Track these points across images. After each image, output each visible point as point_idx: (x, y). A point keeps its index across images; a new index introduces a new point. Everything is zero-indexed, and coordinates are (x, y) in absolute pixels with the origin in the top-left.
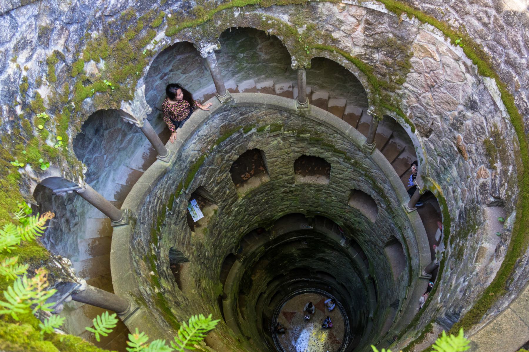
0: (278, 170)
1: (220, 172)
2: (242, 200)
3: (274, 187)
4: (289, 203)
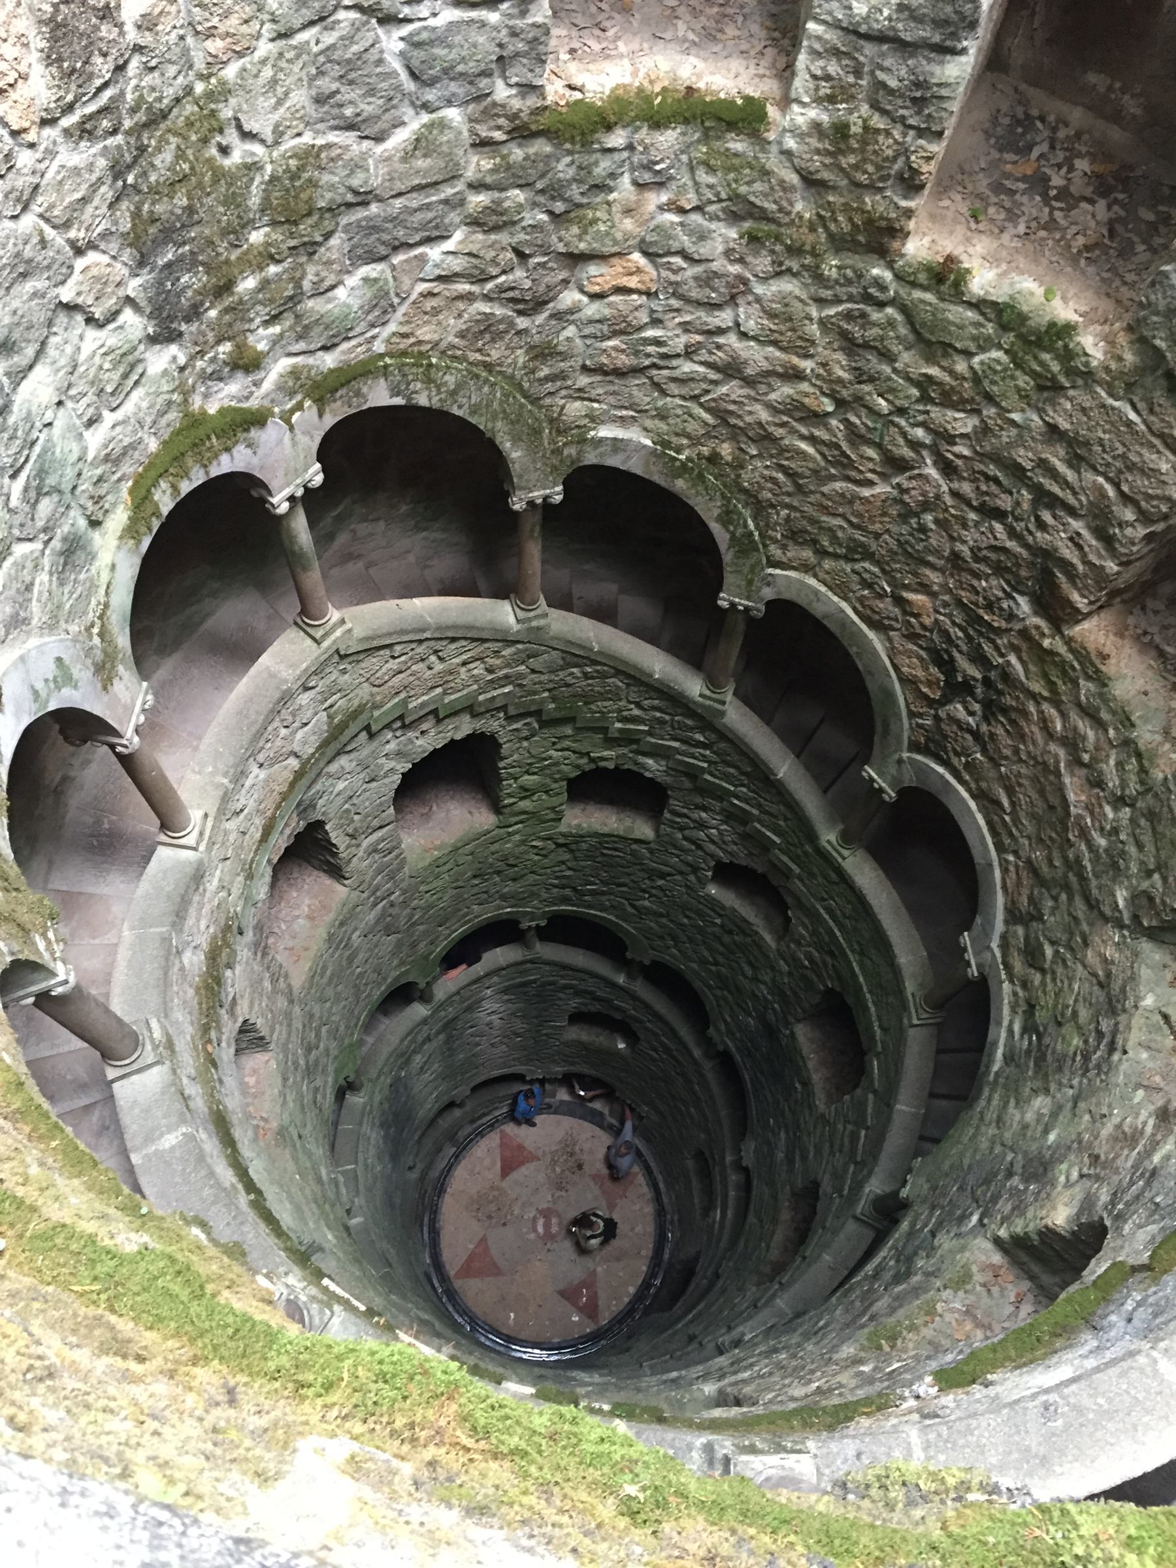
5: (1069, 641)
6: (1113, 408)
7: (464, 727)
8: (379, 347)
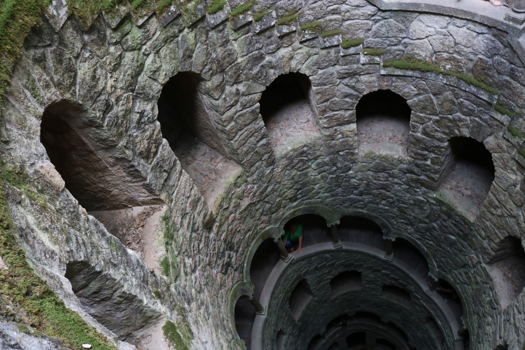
0: (488, 223)
1: (437, 121)
2: (435, 199)
3: (470, 237)
4: (466, 280)
5: (218, 214)
6: (175, 200)
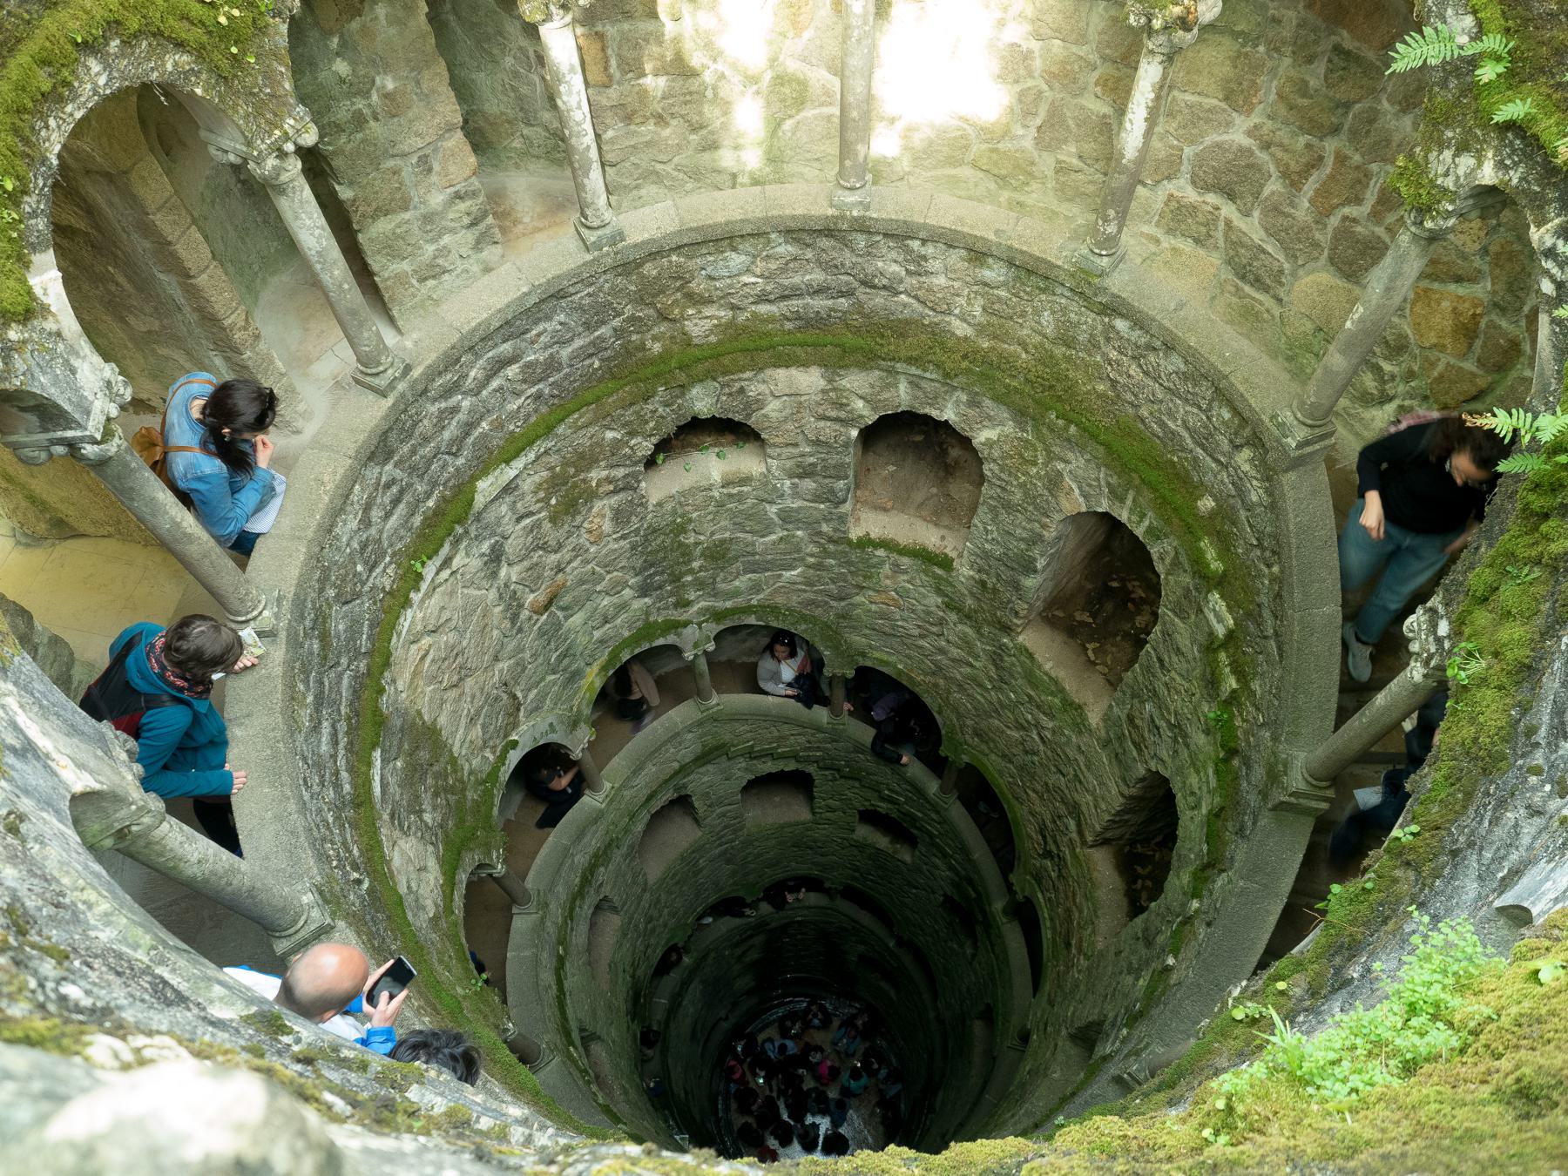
7: (791, 766)
8: (754, 602)
